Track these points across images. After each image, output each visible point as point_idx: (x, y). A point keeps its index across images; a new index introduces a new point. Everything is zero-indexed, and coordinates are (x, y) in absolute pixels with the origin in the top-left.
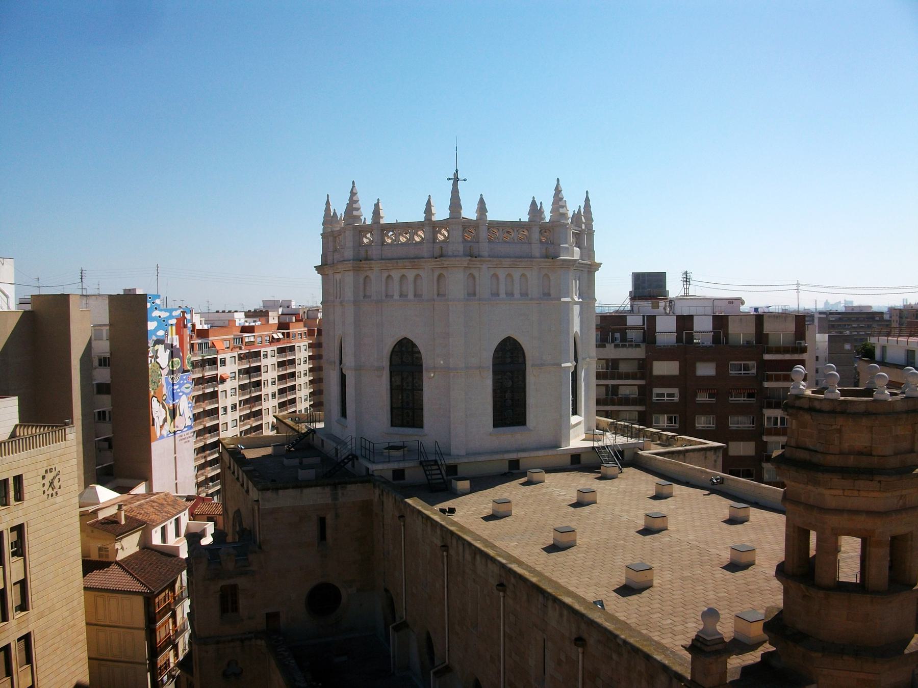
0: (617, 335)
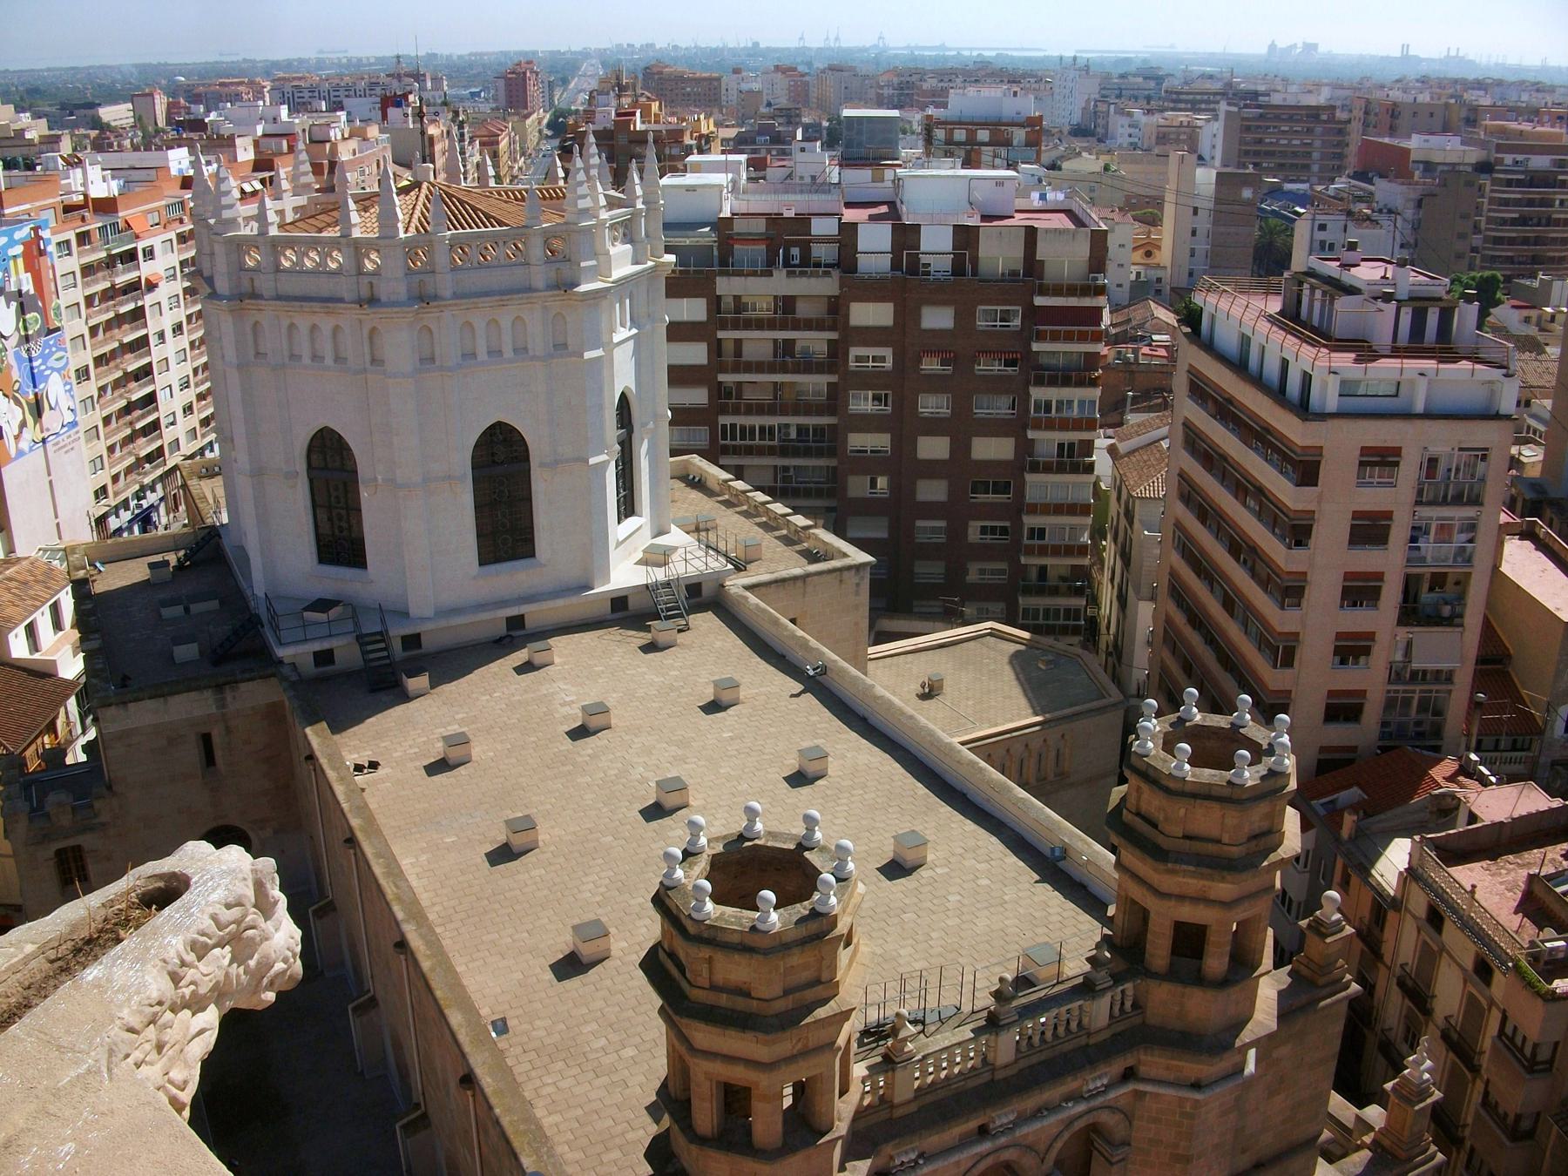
0: (795, 251)
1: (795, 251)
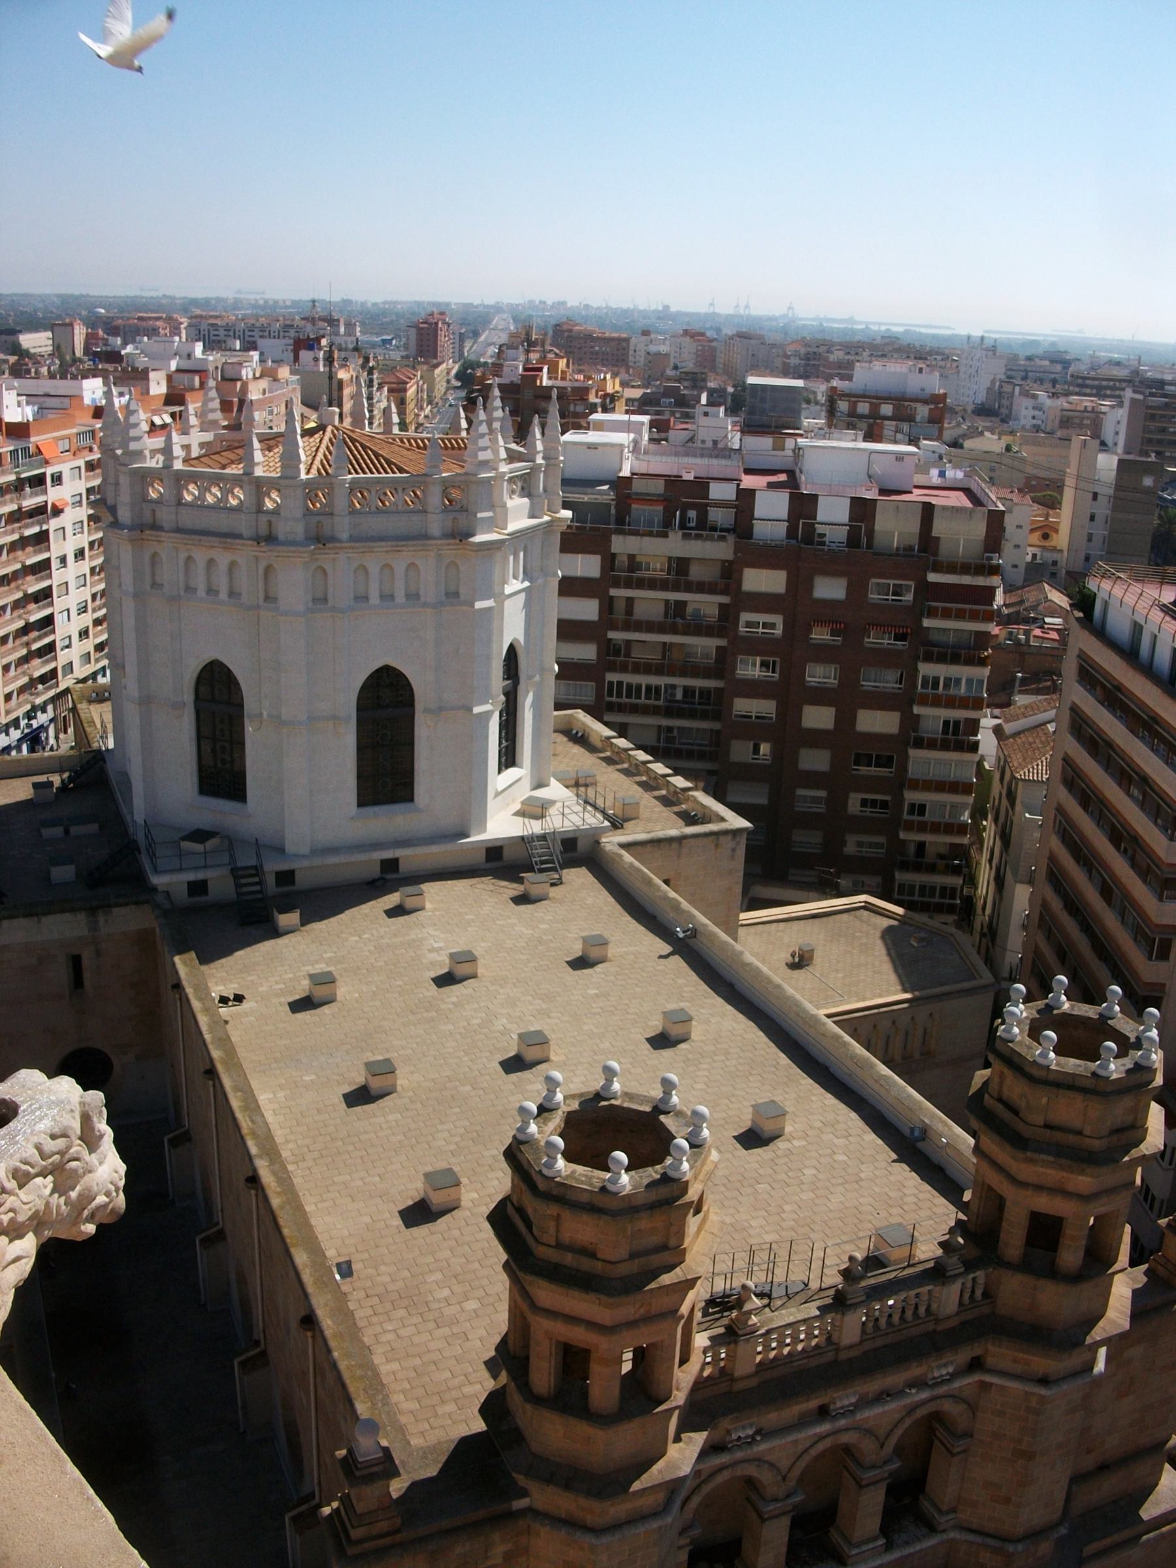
0: (692, 514)
1: (692, 514)
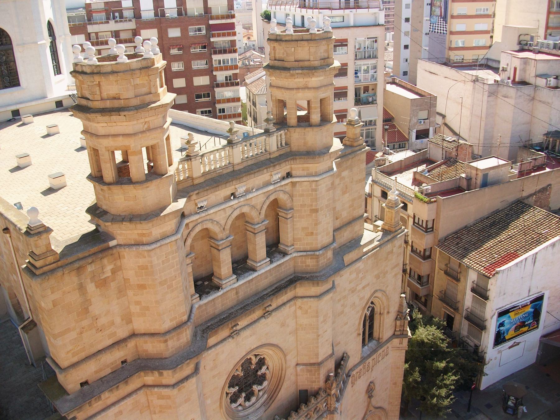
0: (117, 14)
1: (117, 14)
